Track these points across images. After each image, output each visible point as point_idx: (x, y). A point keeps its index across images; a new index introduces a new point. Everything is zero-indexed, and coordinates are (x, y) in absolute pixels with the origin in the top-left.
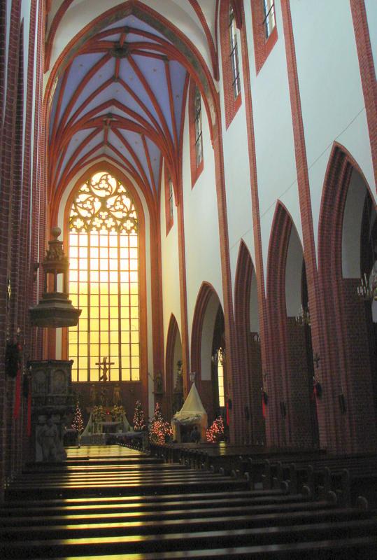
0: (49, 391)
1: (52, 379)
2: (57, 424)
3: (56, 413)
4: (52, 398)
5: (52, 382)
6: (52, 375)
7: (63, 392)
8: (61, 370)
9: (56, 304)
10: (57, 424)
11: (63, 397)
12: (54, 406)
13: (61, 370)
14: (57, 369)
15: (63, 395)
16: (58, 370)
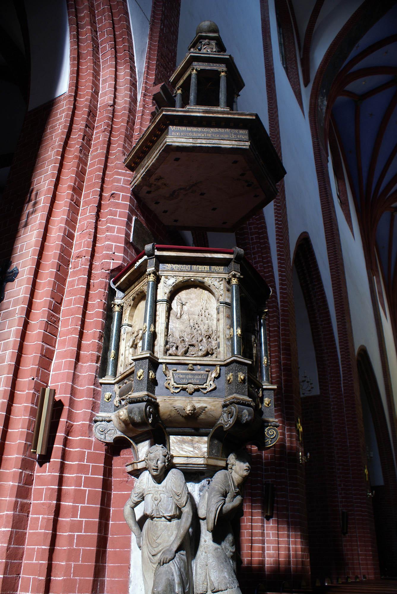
13: (201, 285)
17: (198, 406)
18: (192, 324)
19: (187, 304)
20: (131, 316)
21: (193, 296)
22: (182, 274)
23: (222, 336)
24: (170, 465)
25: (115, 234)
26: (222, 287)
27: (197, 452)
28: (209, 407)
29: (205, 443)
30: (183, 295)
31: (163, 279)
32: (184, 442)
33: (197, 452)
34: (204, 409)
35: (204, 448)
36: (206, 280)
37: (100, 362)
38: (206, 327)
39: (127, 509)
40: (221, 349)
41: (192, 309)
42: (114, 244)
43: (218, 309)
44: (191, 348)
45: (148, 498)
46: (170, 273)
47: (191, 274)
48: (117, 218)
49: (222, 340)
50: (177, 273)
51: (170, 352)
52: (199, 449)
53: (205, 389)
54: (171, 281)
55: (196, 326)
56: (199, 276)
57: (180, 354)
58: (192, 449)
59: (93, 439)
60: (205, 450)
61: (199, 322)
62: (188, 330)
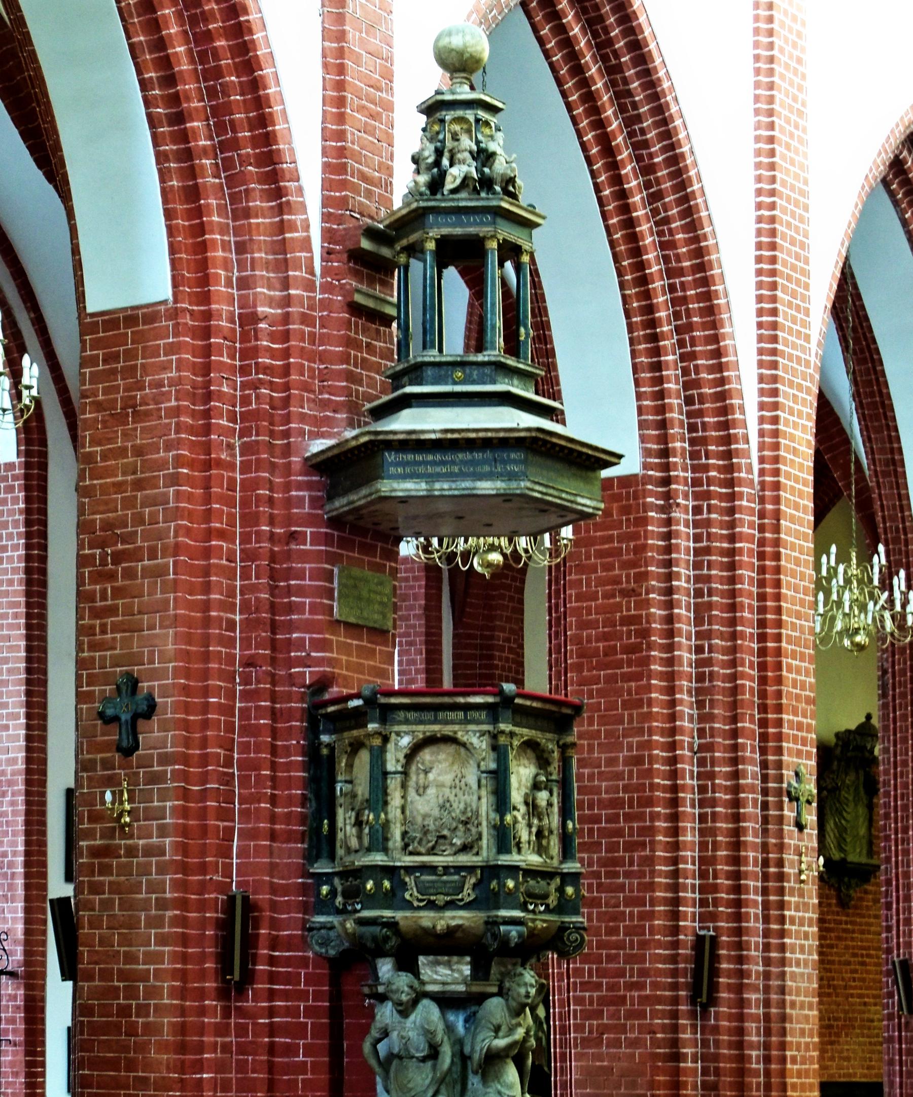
0: (380, 842)
1: (394, 784)
2: (447, 1001)
3: (447, 944)
4: (390, 871)
5: (395, 800)
6: (391, 766)
7: (465, 848)
8: (451, 740)
9: (406, 413)
10: (447, 1001)
11: (458, 869)
12: (399, 915)
13: (451, 740)
14: (423, 730)
15: (464, 859)
16: (430, 741)
17: (453, 923)
18: (441, 801)
19: (434, 771)
20: (350, 766)
21: (442, 756)
22: (421, 728)
23: (484, 823)
24: (419, 996)
25: (307, 616)
26: (484, 746)
27: (456, 975)
28: (466, 923)
29: (467, 964)
30: (426, 755)
31: (393, 736)
32: (438, 963)
33: (456, 975)
34: (459, 927)
35: (467, 970)
36: (459, 735)
37: (307, 840)
38: (462, 806)
39: (367, 1047)
40: (484, 842)
41: (441, 778)
42: (307, 636)
43: (479, 781)
44: (441, 841)
45: (394, 1035)
46: (404, 728)
47: (436, 728)
48: (308, 582)
49: (484, 829)
50: (414, 728)
51: (411, 848)
52: (460, 972)
53: (462, 900)
54: (405, 741)
55: (448, 805)
56: (448, 730)
57: (423, 850)
58: (449, 972)
59: (310, 954)
60: (468, 972)
61: (452, 798)
62: (436, 812)
